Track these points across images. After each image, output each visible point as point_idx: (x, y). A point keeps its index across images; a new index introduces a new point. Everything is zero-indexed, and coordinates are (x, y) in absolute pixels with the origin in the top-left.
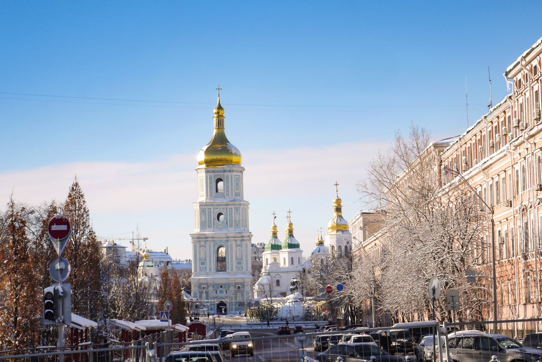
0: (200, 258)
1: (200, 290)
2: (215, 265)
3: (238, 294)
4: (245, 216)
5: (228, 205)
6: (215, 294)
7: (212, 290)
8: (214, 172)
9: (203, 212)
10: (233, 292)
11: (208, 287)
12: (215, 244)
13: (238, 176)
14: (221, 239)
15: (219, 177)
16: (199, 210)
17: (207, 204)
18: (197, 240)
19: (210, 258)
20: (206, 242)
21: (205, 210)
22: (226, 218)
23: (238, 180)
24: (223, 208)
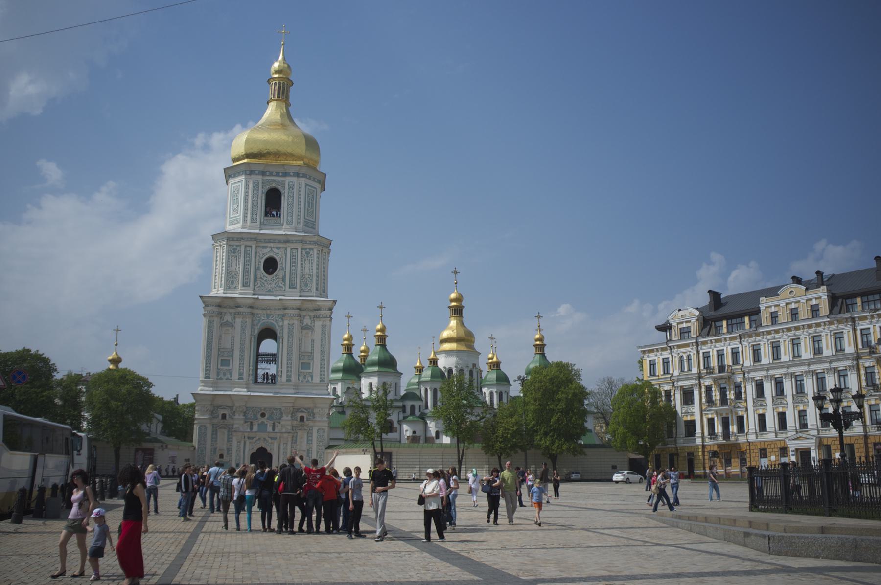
0: (219, 349)
1: (215, 421)
2: (251, 368)
3: (299, 433)
4: (323, 269)
7: (242, 422)
8: (263, 173)
9: (234, 253)
12: (255, 322)
13: (313, 189)
14: (268, 312)
15: (274, 185)
16: (225, 248)
17: (244, 236)
18: (216, 309)
21: (238, 249)
23: (313, 196)
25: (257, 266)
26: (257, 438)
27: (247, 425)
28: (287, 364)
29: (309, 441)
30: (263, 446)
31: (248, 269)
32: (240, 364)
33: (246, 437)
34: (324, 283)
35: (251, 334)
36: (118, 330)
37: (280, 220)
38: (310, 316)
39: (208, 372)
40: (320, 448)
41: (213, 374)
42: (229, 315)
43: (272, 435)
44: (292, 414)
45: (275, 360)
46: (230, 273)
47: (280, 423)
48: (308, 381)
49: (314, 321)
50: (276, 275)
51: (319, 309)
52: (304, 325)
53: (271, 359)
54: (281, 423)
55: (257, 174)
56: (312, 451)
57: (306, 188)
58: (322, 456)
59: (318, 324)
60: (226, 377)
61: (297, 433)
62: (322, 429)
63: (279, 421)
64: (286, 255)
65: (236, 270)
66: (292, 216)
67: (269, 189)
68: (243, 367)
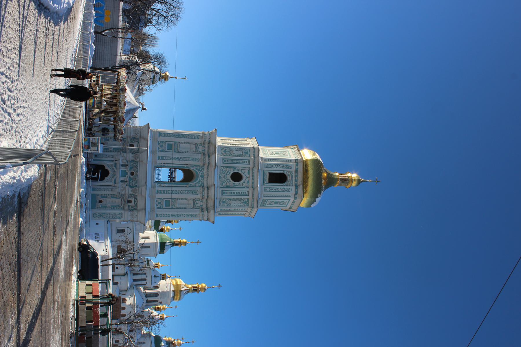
1: (129, 140)
5: (254, 189)
6: (121, 163)
7: (128, 159)
8: (296, 171)
9: (245, 153)
10: (123, 193)
11: (133, 153)
12: (198, 167)
14: (205, 176)
15: (289, 178)
16: (248, 146)
17: (256, 159)
19: (178, 159)
20: (202, 154)
22: (235, 186)
23: (282, 204)
24: (248, 181)
25: (236, 168)
26: (116, 170)
27: (125, 163)
28: (169, 191)
29: (113, 208)
30: (110, 174)
31: (235, 162)
32: (169, 157)
33: (116, 162)
34: (225, 214)
35: (189, 164)
36: (185, 79)
37: (266, 183)
38: (202, 205)
39: (163, 135)
40: (108, 216)
41: (162, 139)
42: (203, 149)
43: (118, 181)
44: (133, 194)
45: (171, 181)
46: (231, 150)
47: (127, 186)
48: (157, 205)
49: (199, 208)
50: (230, 181)
51: (208, 212)
52: (196, 201)
53: (172, 178)
54: (127, 187)
55: (296, 167)
56: (106, 209)
57: (287, 200)
58: (102, 217)
59: (198, 212)
60: (160, 147)
61: (119, 198)
62: (121, 217)
63: (128, 184)
64: (244, 187)
65: (234, 154)
66: (269, 191)
67: (287, 176)
68: (167, 160)
